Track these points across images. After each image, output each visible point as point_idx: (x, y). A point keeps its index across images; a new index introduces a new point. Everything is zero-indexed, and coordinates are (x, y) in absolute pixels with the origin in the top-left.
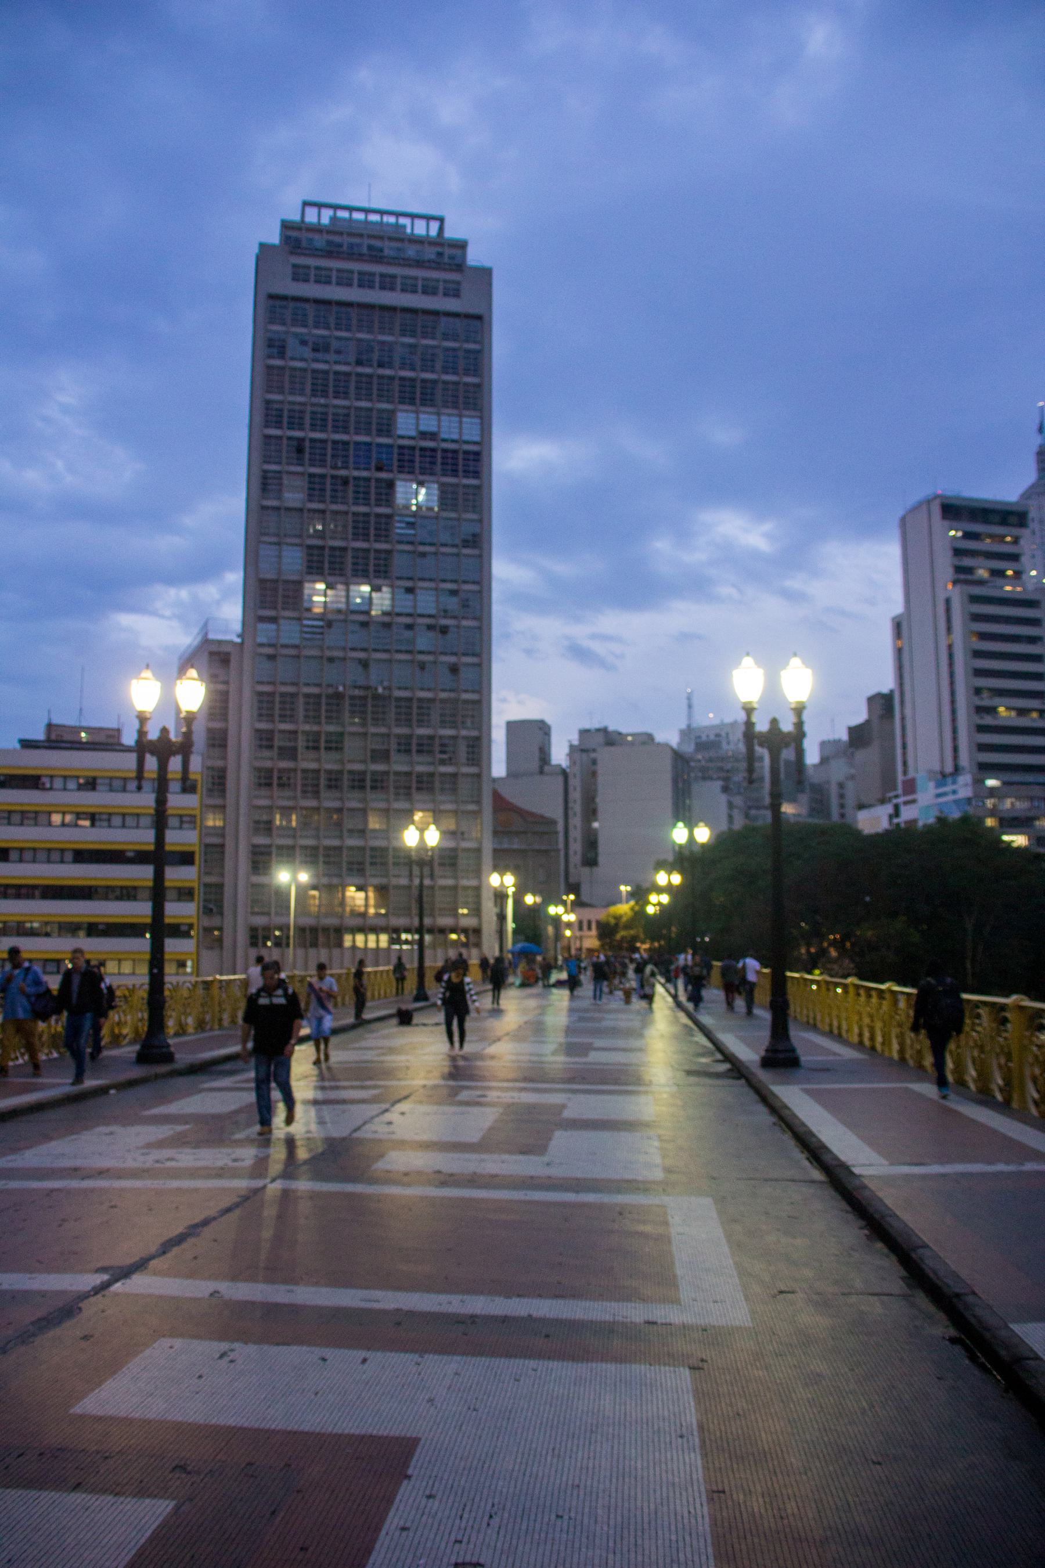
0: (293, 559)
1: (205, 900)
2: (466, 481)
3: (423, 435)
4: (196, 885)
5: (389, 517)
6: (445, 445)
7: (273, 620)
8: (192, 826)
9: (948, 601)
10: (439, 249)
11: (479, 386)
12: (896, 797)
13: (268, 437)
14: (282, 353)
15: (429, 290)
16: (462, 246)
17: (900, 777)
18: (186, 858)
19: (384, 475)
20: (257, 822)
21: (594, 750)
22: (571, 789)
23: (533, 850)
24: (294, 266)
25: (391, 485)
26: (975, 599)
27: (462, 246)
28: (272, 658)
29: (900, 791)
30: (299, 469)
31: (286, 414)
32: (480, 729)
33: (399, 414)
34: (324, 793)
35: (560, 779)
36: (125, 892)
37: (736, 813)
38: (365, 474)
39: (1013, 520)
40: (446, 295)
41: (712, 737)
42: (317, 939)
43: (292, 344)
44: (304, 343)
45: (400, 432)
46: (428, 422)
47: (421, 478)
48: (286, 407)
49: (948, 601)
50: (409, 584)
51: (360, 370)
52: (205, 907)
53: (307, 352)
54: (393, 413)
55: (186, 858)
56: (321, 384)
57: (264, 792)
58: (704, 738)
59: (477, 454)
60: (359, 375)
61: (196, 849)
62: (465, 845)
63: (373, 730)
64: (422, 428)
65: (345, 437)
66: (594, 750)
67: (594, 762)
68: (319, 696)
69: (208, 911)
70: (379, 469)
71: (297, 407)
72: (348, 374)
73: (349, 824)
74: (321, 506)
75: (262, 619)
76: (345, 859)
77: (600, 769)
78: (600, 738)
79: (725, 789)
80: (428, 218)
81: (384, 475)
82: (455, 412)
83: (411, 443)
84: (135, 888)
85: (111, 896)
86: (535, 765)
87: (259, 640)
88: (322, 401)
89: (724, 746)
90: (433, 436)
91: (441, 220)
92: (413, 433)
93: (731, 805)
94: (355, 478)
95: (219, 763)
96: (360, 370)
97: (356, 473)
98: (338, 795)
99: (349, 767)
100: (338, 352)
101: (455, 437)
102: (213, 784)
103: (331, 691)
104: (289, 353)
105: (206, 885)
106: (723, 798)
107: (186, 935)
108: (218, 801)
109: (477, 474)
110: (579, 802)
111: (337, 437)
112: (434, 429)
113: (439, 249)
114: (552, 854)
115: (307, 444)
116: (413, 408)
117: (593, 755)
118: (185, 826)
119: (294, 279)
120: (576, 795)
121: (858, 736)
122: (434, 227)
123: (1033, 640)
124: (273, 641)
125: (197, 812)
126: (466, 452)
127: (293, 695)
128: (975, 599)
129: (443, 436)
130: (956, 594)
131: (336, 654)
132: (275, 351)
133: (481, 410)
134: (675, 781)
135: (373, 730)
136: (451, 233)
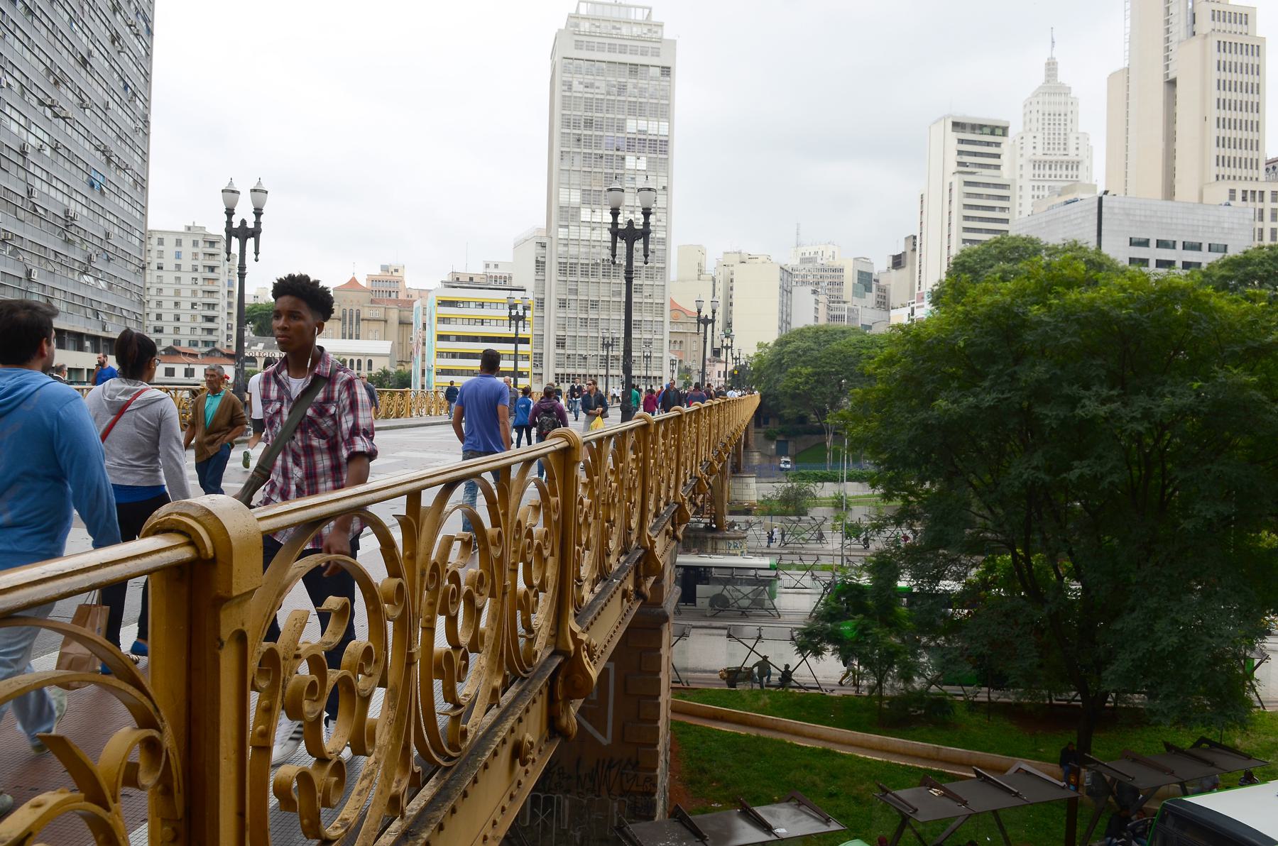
0: (576, 197)
2: (660, 156)
3: (640, 132)
5: (622, 174)
6: (650, 137)
7: (567, 227)
9: (951, 184)
10: (650, 27)
11: (668, 105)
12: (913, 303)
13: (563, 133)
14: (570, 89)
15: (644, 53)
16: (661, 26)
17: (917, 291)
18: (526, 341)
19: (620, 153)
21: (732, 266)
24: (576, 41)
25: (623, 159)
26: (967, 183)
27: (661, 26)
28: (566, 245)
29: (915, 300)
30: (578, 150)
31: (572, 121)
32: (665, 281)
33: (628, 121)
34: (590, 312)
35: (711, 283)
37: (821, 306)
38: (611, 153)
39: (999, 131)
40: (652, 55)
41: (812, 255)
43: (575, 83)
44: (581, 83)
45: (628, 131)
46: (642, 124)
47: (638, 155)
48: (572, 117)
49: (951, 184)
50: (632, 209)
51: (608, 97)
53: (581, 88)
54: (625, 120)
55: (526, 341)
56: (589, 105)
57: (562, 310)
58: (807, 255)
59: (666, 141)
60: (608, 100)
62: (655, 337)
63: (613, 281)
64: (639, 128)
65: (601, 133)
66: (732, 266)
67: (732, 274)
68: (588, 264)
69: (536, 366)
70: (618, 150)
71: (577, 118)
72: (602, 100)
73: (602, 325)
74: (589, 169)
75: (561, 226)
77: (734, 277)
78: (737, 258)
79: (815, 292)
80: (644, 8)
81: (620, 153)
82: (656, 119)
83: (634, 136)
86: (696, 273)
87: (560, 237)
88: (590, 114)
89: (819, 261)
90: (644, 132)
91: (650, 9)
92: (635, 131)
93: (817, 302)
94: (606, 155)
95: (541, 296)
96: (608, 97)
97: (606, 152)
99: (602, 299)
100: (598, 88)
101: (656, 133)
103: (593, 262)
104: (574, 89)
105: (535, 354)
106: (814, 297)
107: (527, 376)
108: (541, 315)
109: (666, 152)
111: (597, 133)
112: (646, 129)
113: (650, 27)
115: (583, 137)
116: (634, 117)
117: (731, 268)
119: (576, 48)
120: (720, 294)
121: (898, 262)
122: (647, 11)
123: (1003, 209)
124: (567, 237)
126: (661, 141)
127: (576, 264)
128: (967, 183)
129: (649, 132)
130: (957, 181)
131: (596, 244)
132: (566, 88)
133: (668, 118)
134: (781, 287)
135: (613, 281)
136: (655, 19)
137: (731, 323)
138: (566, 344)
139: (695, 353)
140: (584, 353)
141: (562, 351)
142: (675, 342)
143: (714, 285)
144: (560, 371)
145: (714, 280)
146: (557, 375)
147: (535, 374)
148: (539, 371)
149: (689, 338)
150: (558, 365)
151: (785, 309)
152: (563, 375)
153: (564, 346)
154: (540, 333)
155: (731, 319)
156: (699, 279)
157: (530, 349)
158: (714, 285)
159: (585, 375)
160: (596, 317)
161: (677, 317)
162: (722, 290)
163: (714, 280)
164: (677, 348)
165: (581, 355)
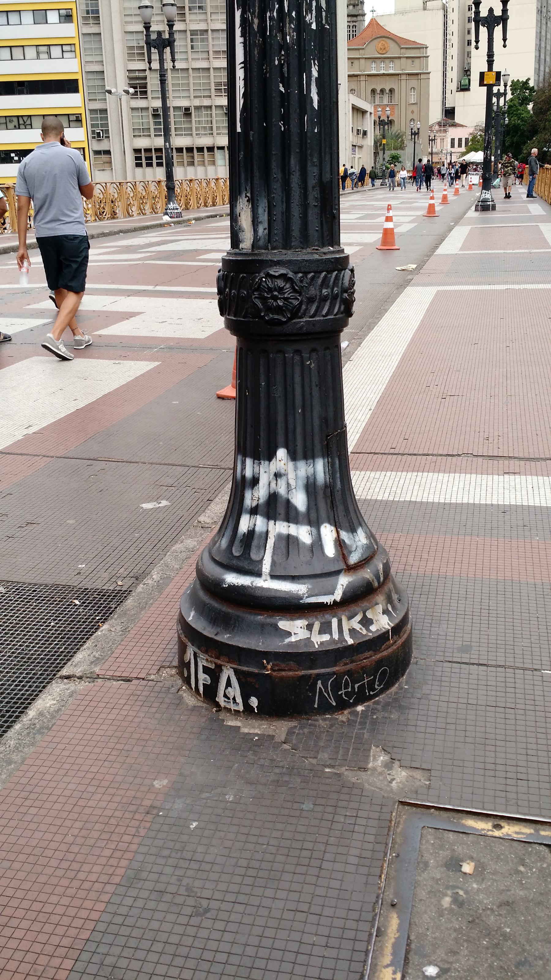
1: (93, 126)
4: (82, 111)
8: (73, 54)
20: (131, 48)
22: (449, 22)
23: (406, 74)
35: (441, 13)
36: (21, 122)
42: (193, 157)
52: (93, 132)
61: (78, 77)
69: (97, 136)
76: (212, 80)
84: (30, 116)
85: (10, 125)
98: (203, 17)
102: (88, 12)
108: (93, 29)
110: (456, 34)
114: (423, 76)
118: (65, 55)
125: (76, 41)
137: (469, 70)
138: (149, 89)
139: (414, 108)
140: (184, 103)
141: (141, 103)
142: (382, 91)
143: (445, 16)
144: (143, 143)
145: (445, 9)
146: (137, 151)
147: (97, 153)
148: (103, 146)
149: (403, 82)
150: (138, 132)
151: (543, 45)
152: (148, 150)
153: (145, 93)
154: (97, 68)
155: (469, 64)
156: (425, 9)
157: (80, 103)
158: (445, 16)
159: (190, 150)
160: (202, 26)
161: (384, 49)
162: (456, 22)
163: (445, 9)
164: (386, 101)
165: (179, 108)
